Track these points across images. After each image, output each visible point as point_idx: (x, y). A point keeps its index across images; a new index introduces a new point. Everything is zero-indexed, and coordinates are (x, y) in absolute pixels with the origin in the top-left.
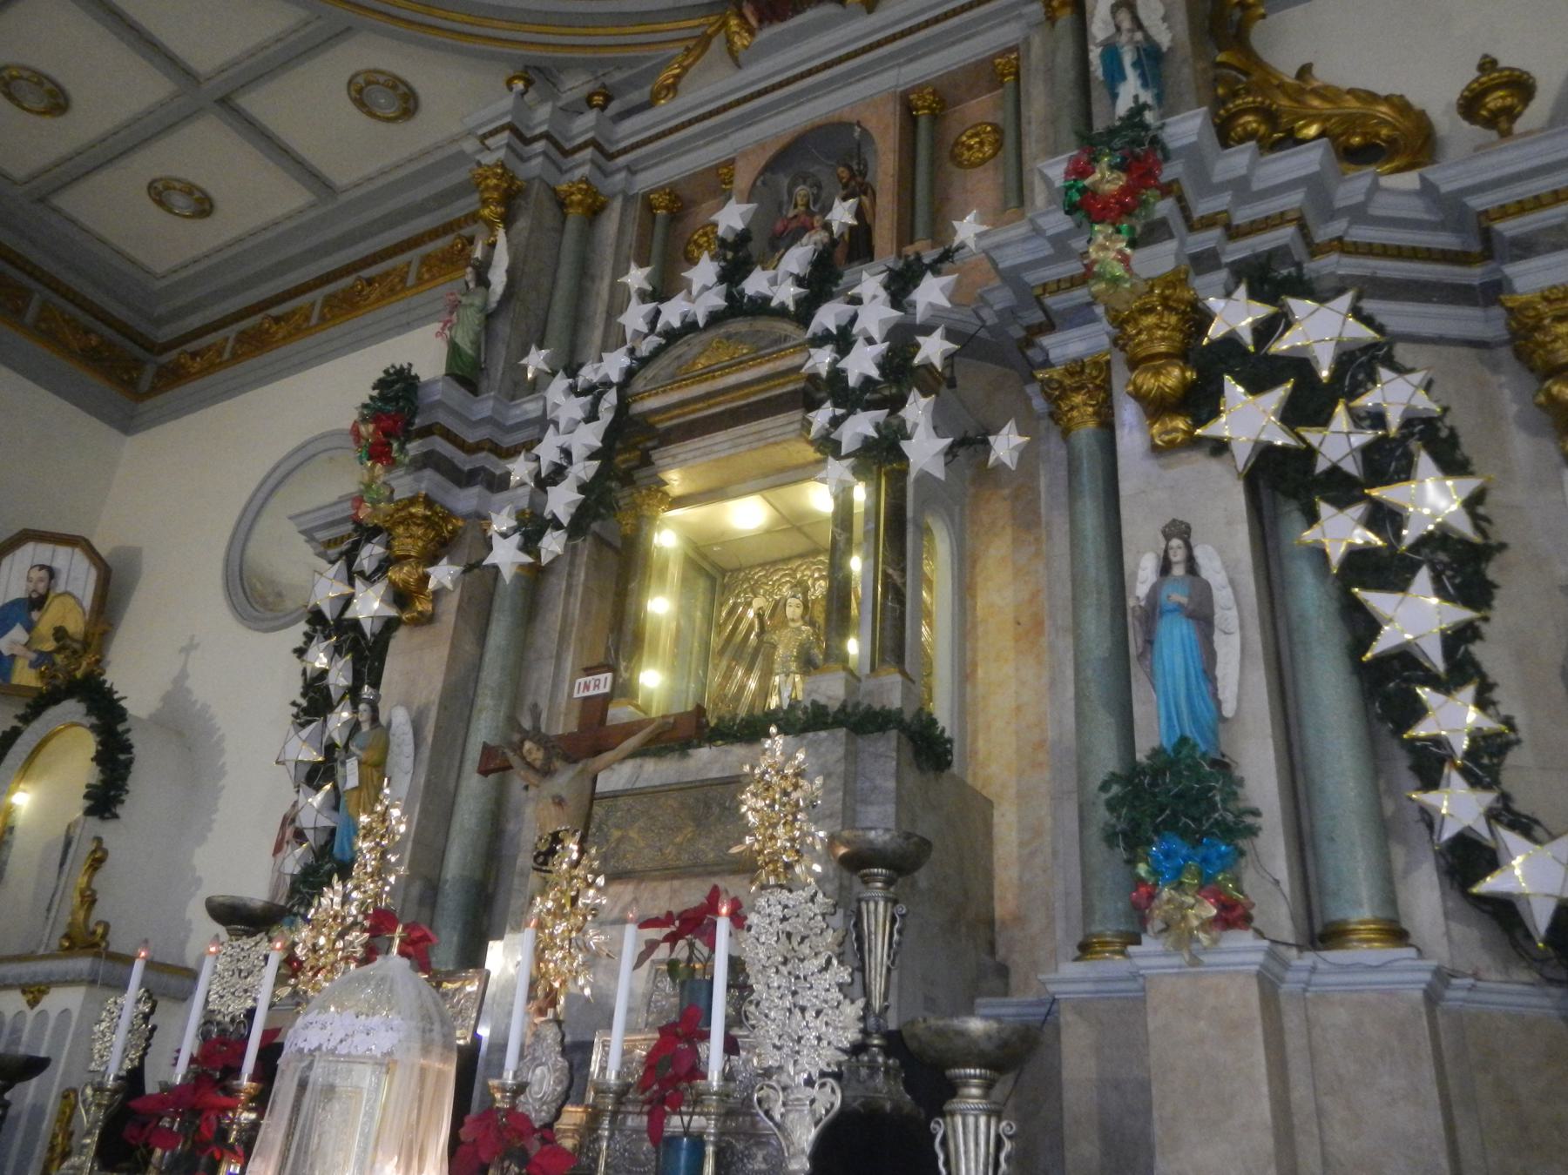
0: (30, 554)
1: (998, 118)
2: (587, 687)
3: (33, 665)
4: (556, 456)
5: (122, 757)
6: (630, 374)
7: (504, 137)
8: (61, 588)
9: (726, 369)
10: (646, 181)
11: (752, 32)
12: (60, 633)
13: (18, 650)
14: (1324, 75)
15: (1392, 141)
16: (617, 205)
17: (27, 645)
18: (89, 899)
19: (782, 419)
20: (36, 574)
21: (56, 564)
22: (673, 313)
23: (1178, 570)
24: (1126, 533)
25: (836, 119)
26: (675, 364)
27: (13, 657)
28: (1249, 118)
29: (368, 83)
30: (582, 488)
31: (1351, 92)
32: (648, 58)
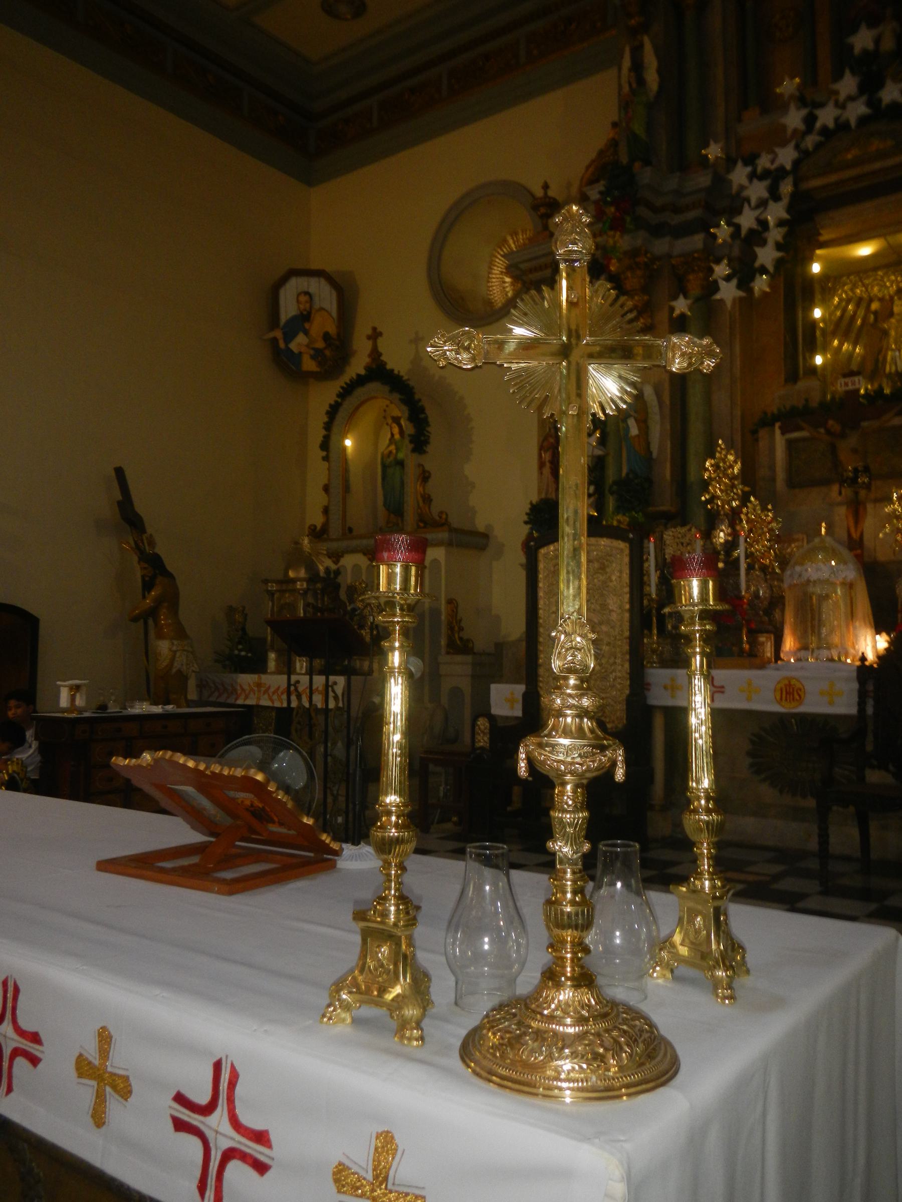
0: (294, 285)
2: (846, 384)
3: (313, 357)
4: (755, 226)
5: (423, 416)
6: (796, 163)
8: (316, 306)
12: (326, 337)
13: (303, 349)
17: (308, 346)
18: (427, 499)
20: (303, 298)
21: (311, 290)
22: (827, 117)
27: (300, 353)
30: (779, 247)
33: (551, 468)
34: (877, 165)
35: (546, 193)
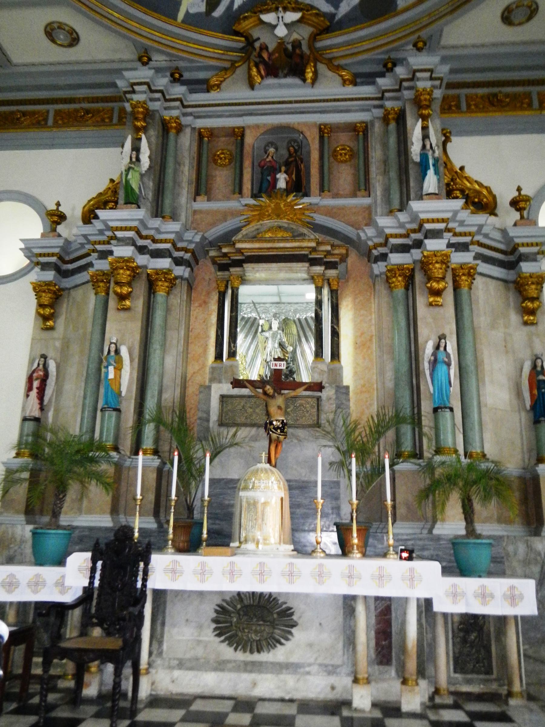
1: (352, 144)
7: (144, 88)
9: (279, 241)
10: (200, 123)
11: (262, 78)
14: (468, 172)
15: (487, 204)
16: (188, 131)
19: (300, 265)
23: (442, 349)
24: (419, 331)
25: (291, 126)
26: (256, 232)
28: (458, 192)
29: (59, 28)
31: (476, 182)
32: (198, 62)
33: (38, 393)
34: (282, 245)
35: (58, 209)
